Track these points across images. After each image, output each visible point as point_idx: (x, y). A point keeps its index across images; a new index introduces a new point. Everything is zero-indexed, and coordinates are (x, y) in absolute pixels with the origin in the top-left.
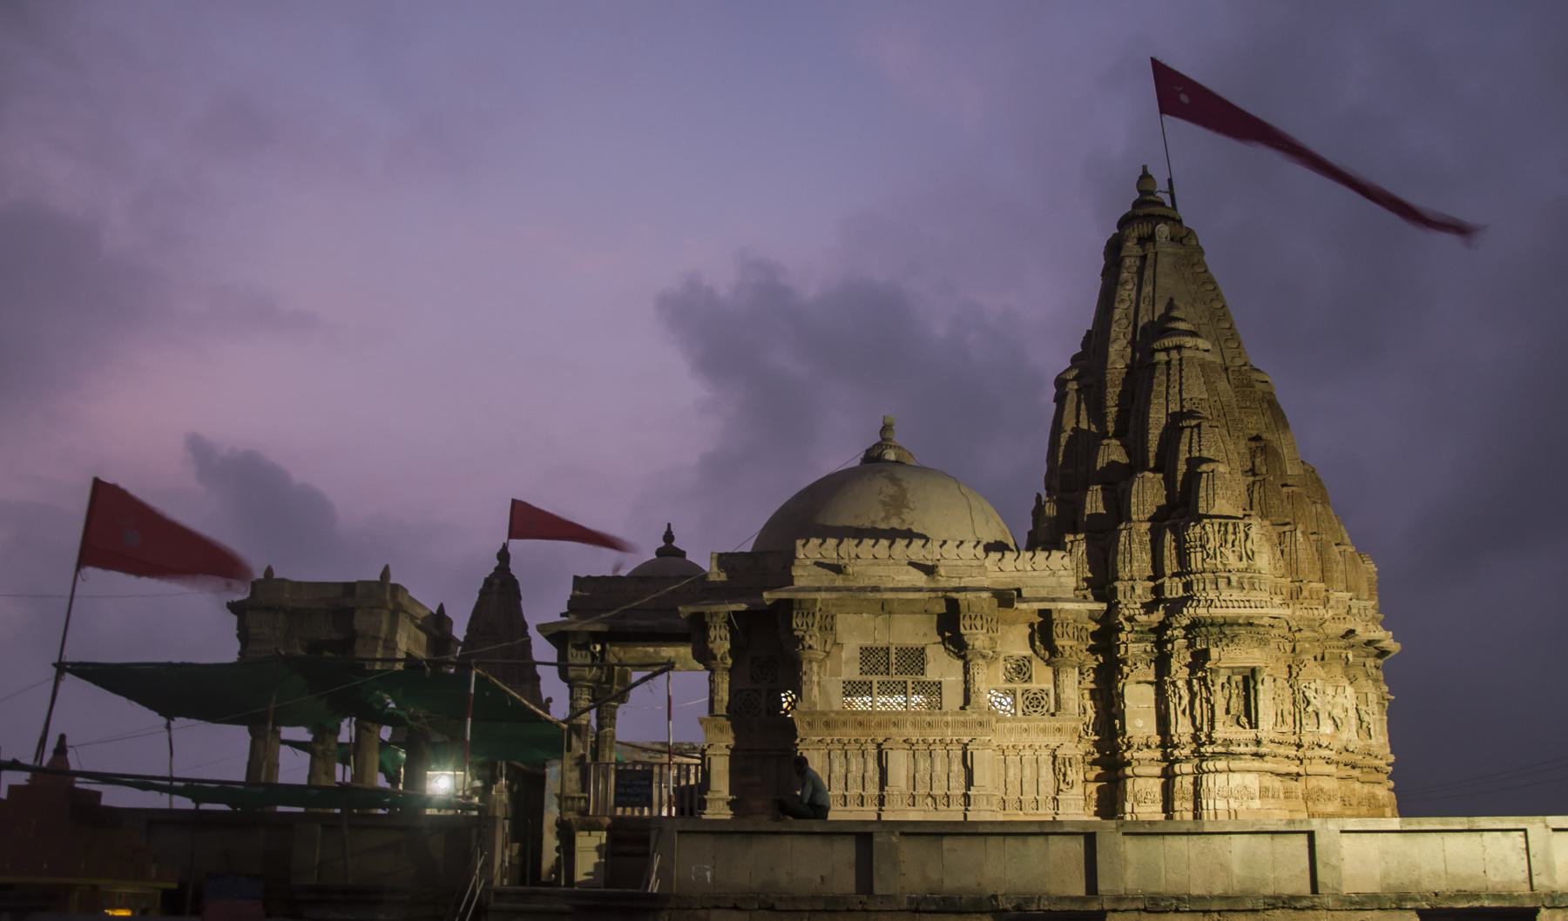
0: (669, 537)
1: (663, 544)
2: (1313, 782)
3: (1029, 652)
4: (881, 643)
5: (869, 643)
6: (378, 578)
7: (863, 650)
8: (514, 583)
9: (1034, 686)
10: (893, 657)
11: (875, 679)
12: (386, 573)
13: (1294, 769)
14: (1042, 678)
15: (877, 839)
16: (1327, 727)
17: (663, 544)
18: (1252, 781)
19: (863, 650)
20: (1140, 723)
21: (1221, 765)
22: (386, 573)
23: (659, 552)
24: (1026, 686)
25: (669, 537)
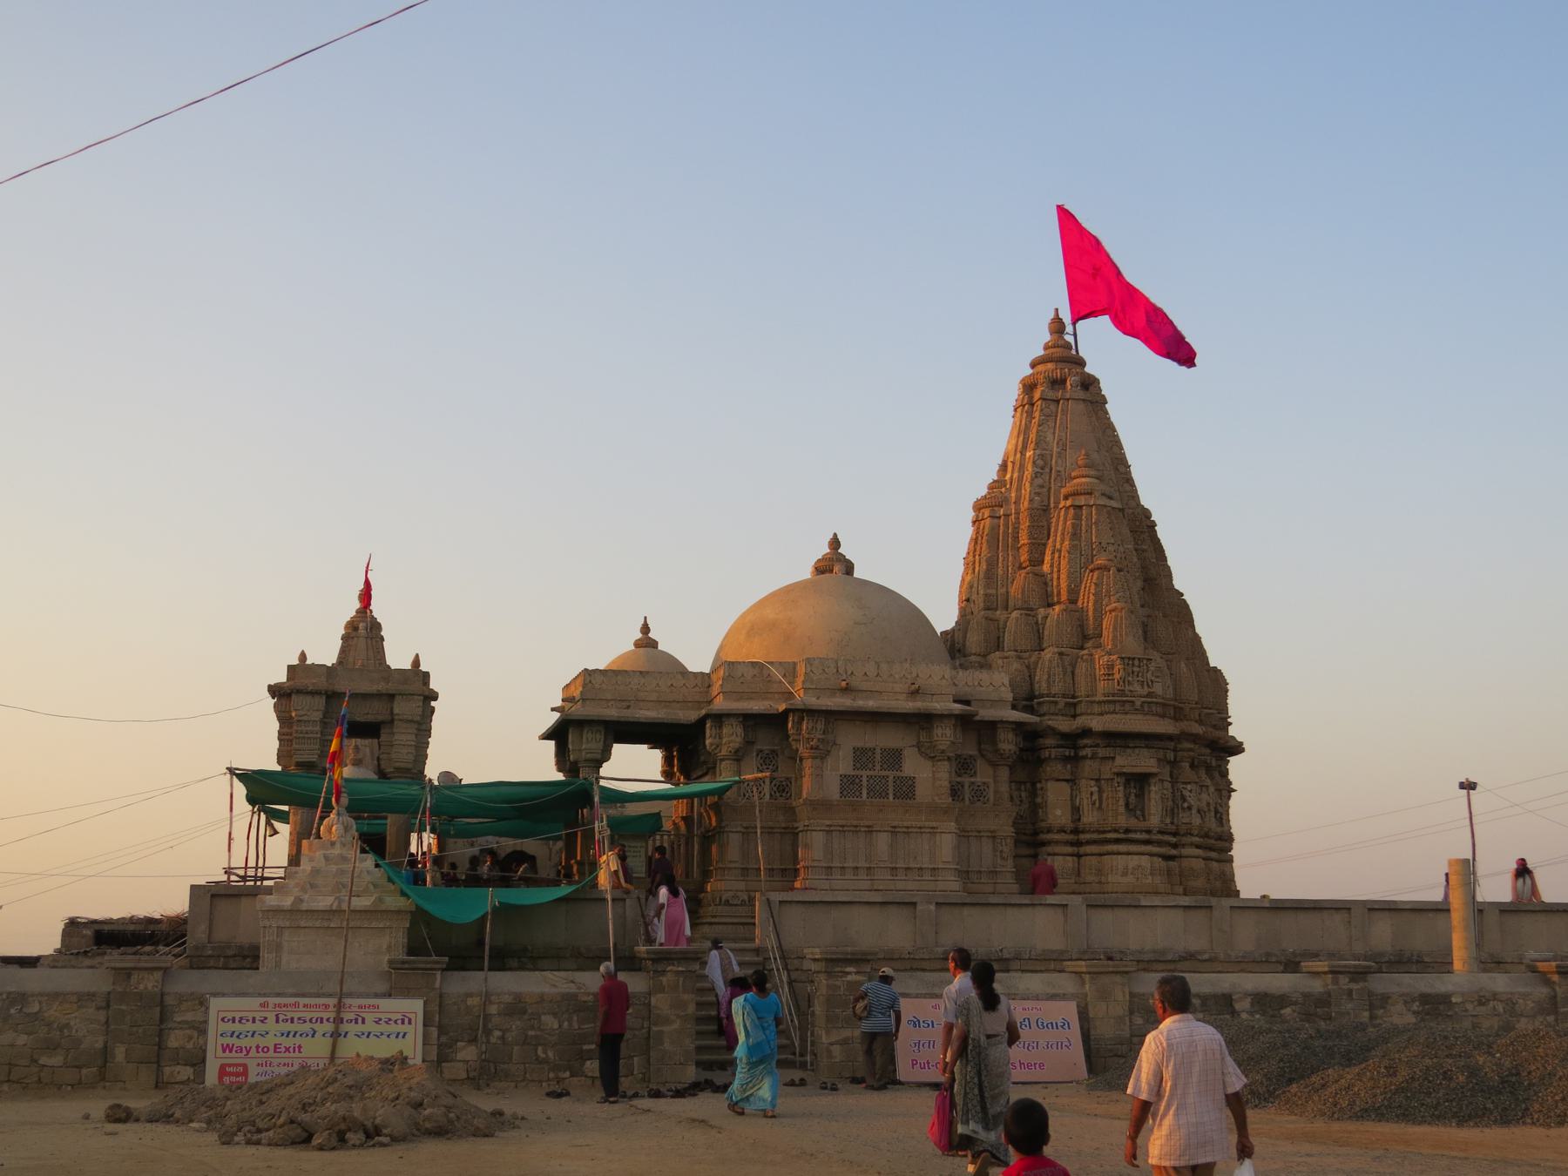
0: (645, 629)
1: (640, 635)
2: (1186, 863)
3: (974, 752)
4: (868, 745)
5: (860, 744)
6: (409, 667)
7: (855, 750)
8: (375, 627)
9: (978, 779)
10: (878, 757)
11: (865, 773)
12: (416, 662)
13: (1174, 852)
14: (983, 774)
15: (919, 907)
16: (1197, 821)
17: (640, 635)
18: (1145, 861)
19: (855, 750)
20: (1059, 812)
21: (1122, 848)
22: (416, 662)
23: (638, 644)
25: (645, 629)
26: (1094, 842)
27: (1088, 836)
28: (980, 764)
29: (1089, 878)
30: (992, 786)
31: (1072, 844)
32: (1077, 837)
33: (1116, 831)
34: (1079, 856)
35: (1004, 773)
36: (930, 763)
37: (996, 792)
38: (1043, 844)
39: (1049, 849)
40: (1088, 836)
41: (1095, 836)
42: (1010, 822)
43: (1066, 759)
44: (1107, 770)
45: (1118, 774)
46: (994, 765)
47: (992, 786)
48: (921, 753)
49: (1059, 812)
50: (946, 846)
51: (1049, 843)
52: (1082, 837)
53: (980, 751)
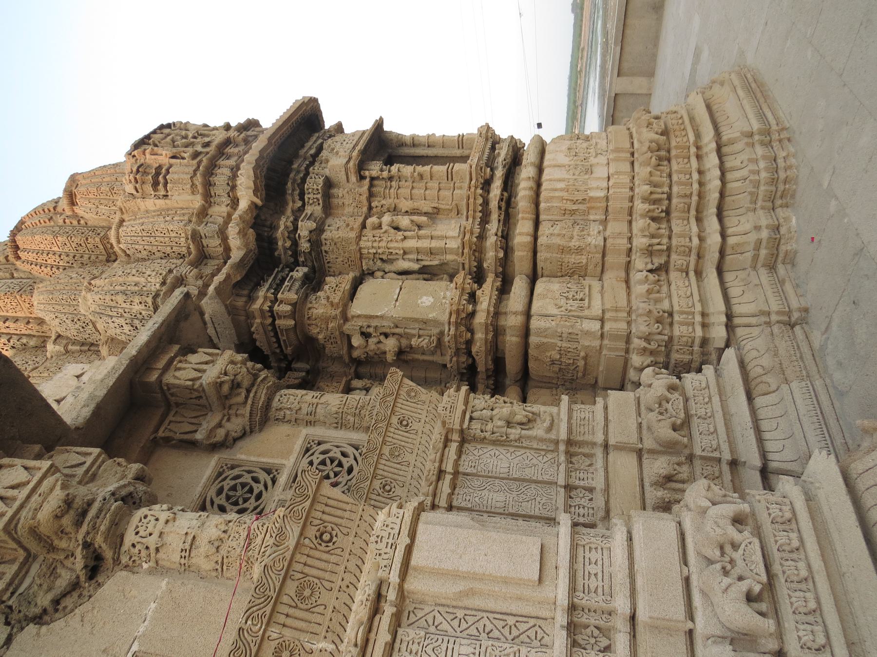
3: (210, 465)
20: (427, 301)
24: (282, 479)
26: (506, 237)
27: (491, 240)
28: (252, 453)
29: (594, 239)
30: (318, 432)
31: (504, 289)
32: (493, 267)
33: (487, 184)
34: (533, 278)
35: (293, 399)
36: (113, 585)
37: (340, 424)
38: (499, 362)
39: (511, 340)
40: (491, 240)
41: (493, 226)
42: (426, 395)
43: (314, 282)
44: (350, 194)
45: (361, 167)
46: (263, 418)
47: (318, 432)
48: (39, 619)
49: (427, 301)
50: (457, 554)
51: (497, 331)
52: (491, 255)
53: (215, 447)
